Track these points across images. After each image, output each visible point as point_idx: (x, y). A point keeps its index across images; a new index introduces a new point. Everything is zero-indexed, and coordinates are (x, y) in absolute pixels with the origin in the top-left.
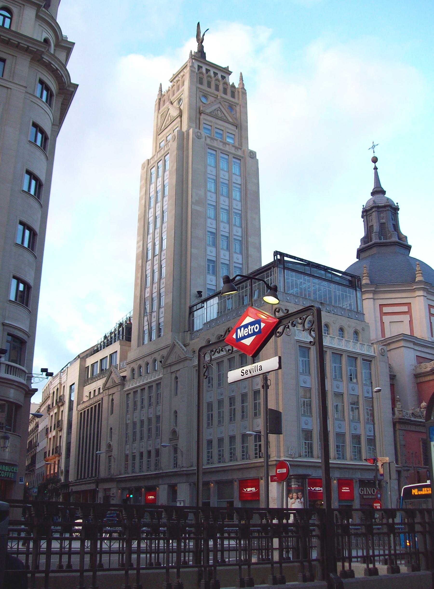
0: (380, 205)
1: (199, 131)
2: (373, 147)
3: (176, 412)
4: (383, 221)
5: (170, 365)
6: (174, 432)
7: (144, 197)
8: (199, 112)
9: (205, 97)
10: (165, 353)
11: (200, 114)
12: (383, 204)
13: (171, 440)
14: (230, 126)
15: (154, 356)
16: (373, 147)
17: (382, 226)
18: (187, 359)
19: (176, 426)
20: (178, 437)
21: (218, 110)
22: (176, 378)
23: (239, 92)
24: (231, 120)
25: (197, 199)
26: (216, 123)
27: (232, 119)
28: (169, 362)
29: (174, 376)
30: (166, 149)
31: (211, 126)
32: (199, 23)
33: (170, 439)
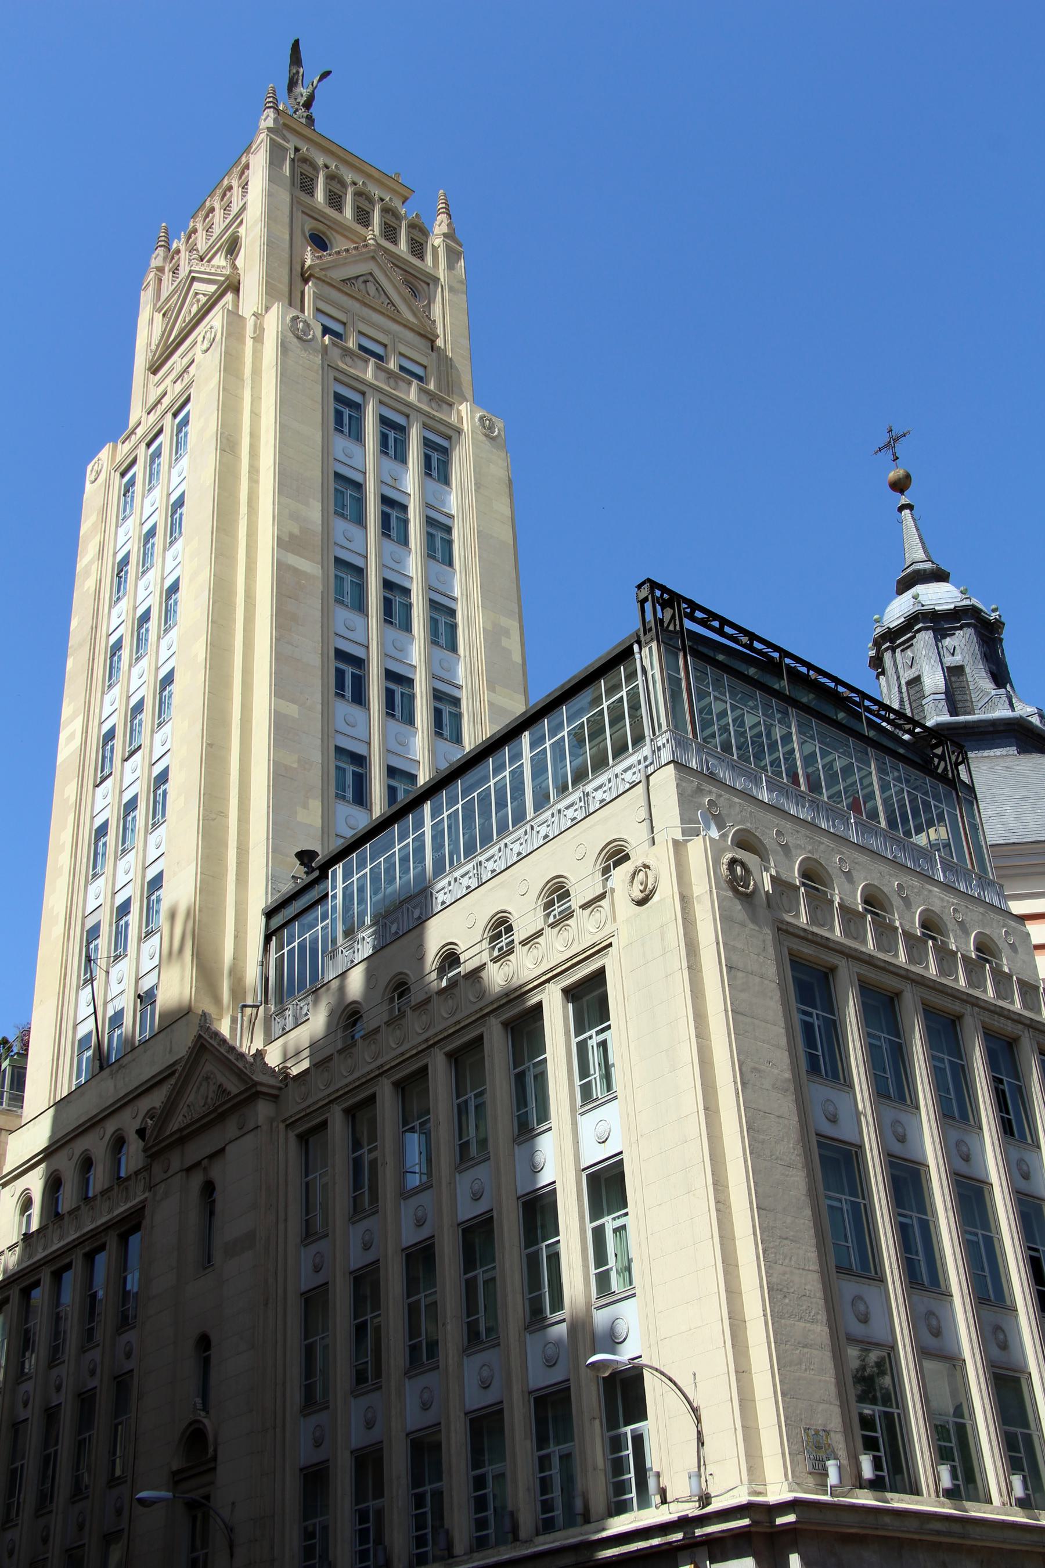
0: (937, 608)
1: (300, 315)
2: (893, 441)
3: (204, 1342)
4: (957, 660)
5: (183, 1138)
6: (196, 1440)
7: (94, 567)
8: (302, 275)
9: (319, 242)
10: (156, 1099)
11: (306, 281)
12: (952, 606)
13: (177, 1479)
14: (410, 336)
15: (111, 1127)
16: (893, 441)
17: (954, 673)
18: (258, 1095)
19: (205, 1408)
20: (215, 1458)
21: (365, 282)
22: (209, 1188)
23: (435, 249)
24: (412, 318)
25: (296, 531)
26: (364, 320)
27: (415, 314)
28: (176, 1123)
29: (197, 1181)
30: (179, 386)
31: (344, 324)
32: (296, 44)
33: (174, 1474)
